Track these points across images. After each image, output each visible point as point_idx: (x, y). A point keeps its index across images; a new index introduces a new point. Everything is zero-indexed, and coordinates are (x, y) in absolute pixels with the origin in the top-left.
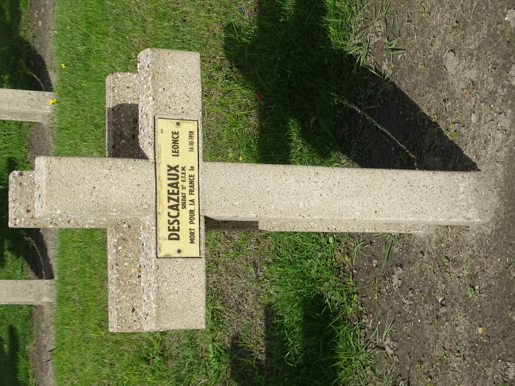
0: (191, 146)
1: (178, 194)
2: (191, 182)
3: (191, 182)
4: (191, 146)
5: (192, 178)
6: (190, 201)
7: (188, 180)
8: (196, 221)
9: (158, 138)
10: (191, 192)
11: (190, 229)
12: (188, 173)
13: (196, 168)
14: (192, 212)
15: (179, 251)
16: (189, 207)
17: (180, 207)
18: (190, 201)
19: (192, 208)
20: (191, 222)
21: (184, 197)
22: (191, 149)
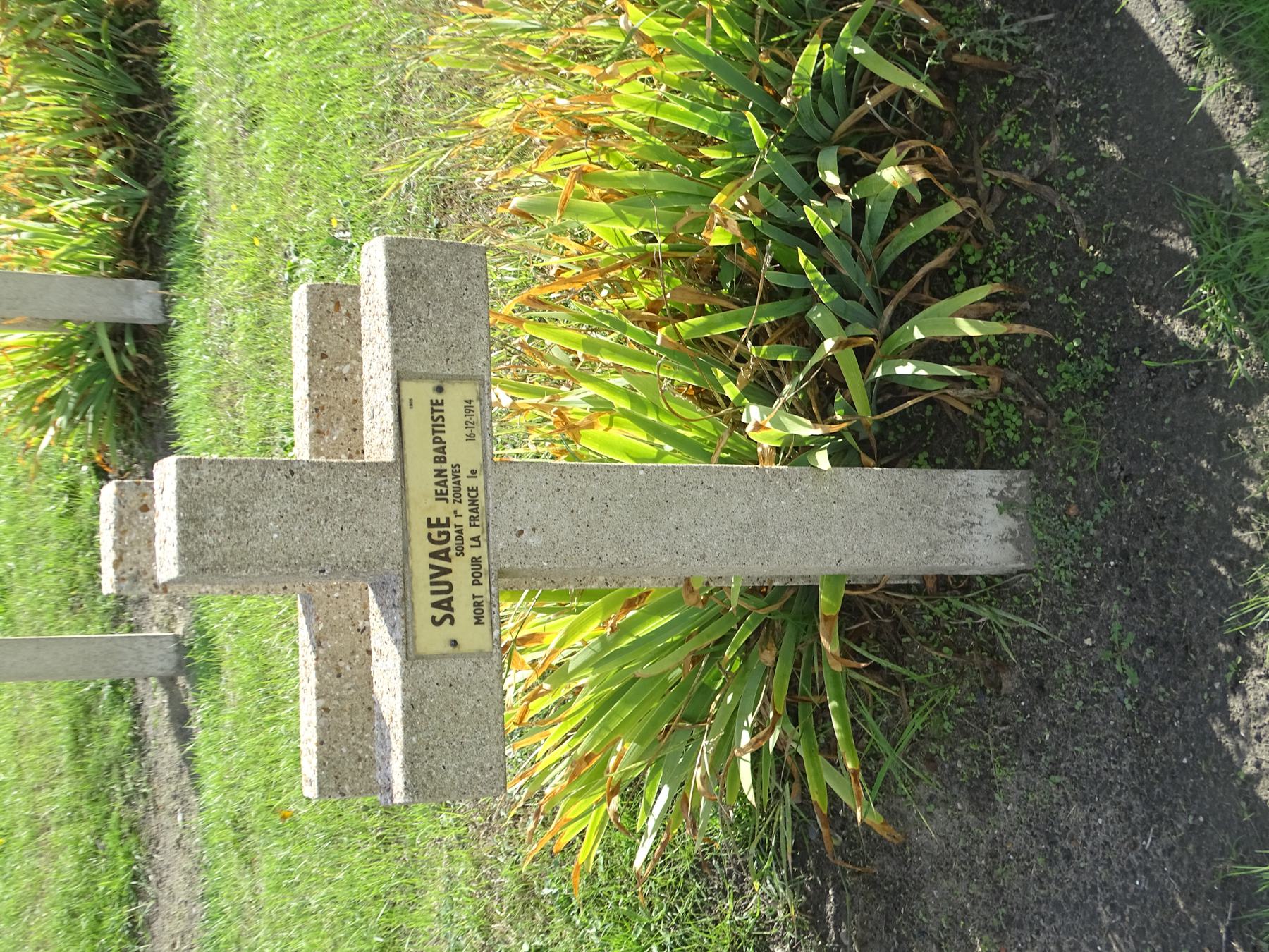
2: (473, 501)
3: (473, 501)
4: (468, 431)
5: (473, 494)
6: (473, 539)
7: (465, 498)
10: (473, 520)
11: (474, 597)
12: (466, 483)
14: (476, 561)
16: (470, 553)
17: (452, 553)
18: (473, 539)
19: (475, 553)
20: (476, 582)
21: (460, 532)
22: (471, 437)
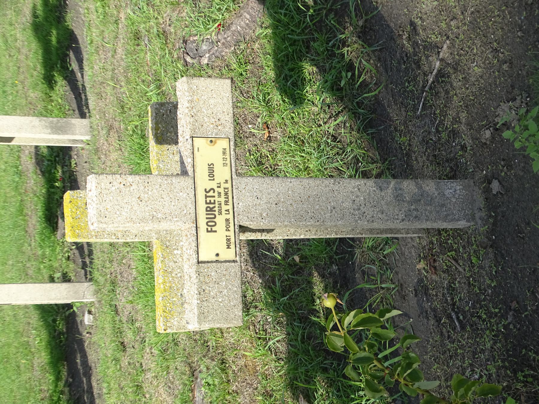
0: (224, 162)
1: (214, 203)
2: (226, 194)
3: (226, 194)
4: (224, 162)
5: (226, 190)
6: (226, 211)
8: (232, 229)
9: (197, 165)
10: (226, 203)
11: (227, 236)
12: (223, 185)
13: (230, 182)
15: (217, 255)
16: (224, 216)
18: (226, 211)
19: (228, 217)
20: (227, 230)
22: (225, 165)
